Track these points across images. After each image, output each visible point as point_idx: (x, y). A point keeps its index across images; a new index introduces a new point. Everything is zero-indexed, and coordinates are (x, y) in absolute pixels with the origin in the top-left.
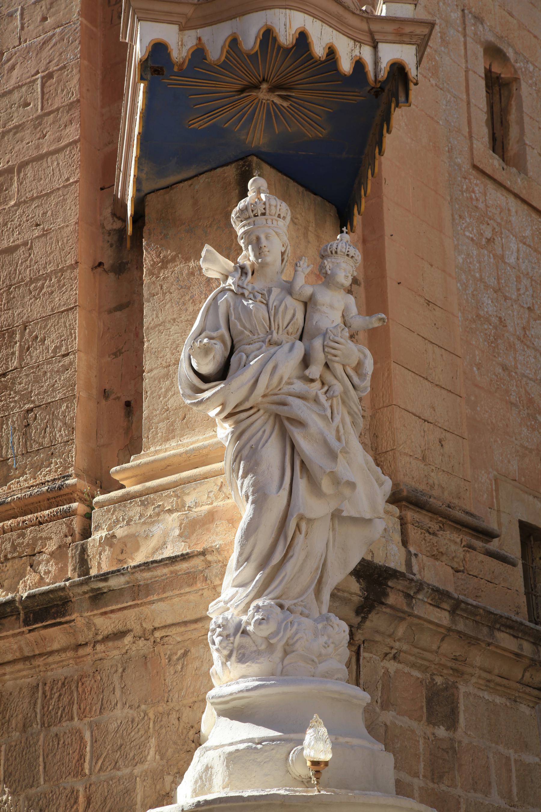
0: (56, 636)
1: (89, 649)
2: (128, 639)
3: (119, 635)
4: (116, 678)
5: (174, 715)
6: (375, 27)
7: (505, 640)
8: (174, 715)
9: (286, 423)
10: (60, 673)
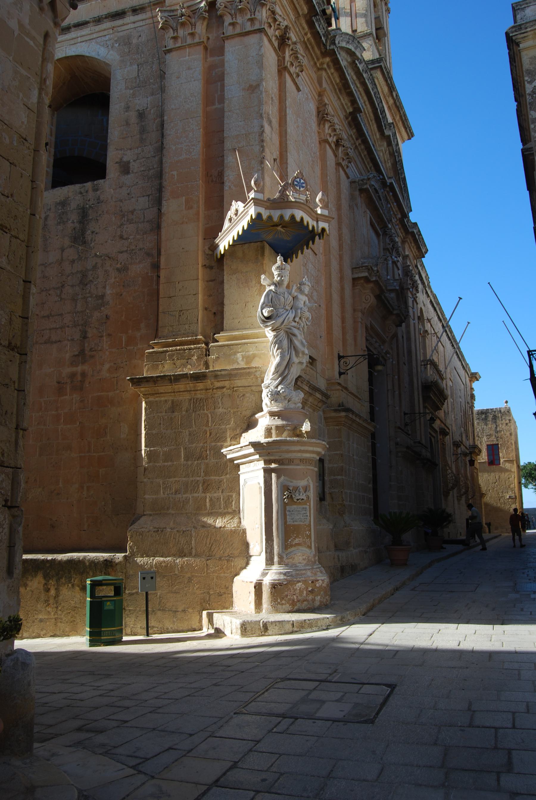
0: (200, 386)
1: (211, 391)
2: (225, 389)
3: (223, 387)
4: (219, 400)
5: (239, 413)
6: (318, 216)
7: (318, 395)
8: (239, 413)
9: (290, 335)
10: (199, 396)
